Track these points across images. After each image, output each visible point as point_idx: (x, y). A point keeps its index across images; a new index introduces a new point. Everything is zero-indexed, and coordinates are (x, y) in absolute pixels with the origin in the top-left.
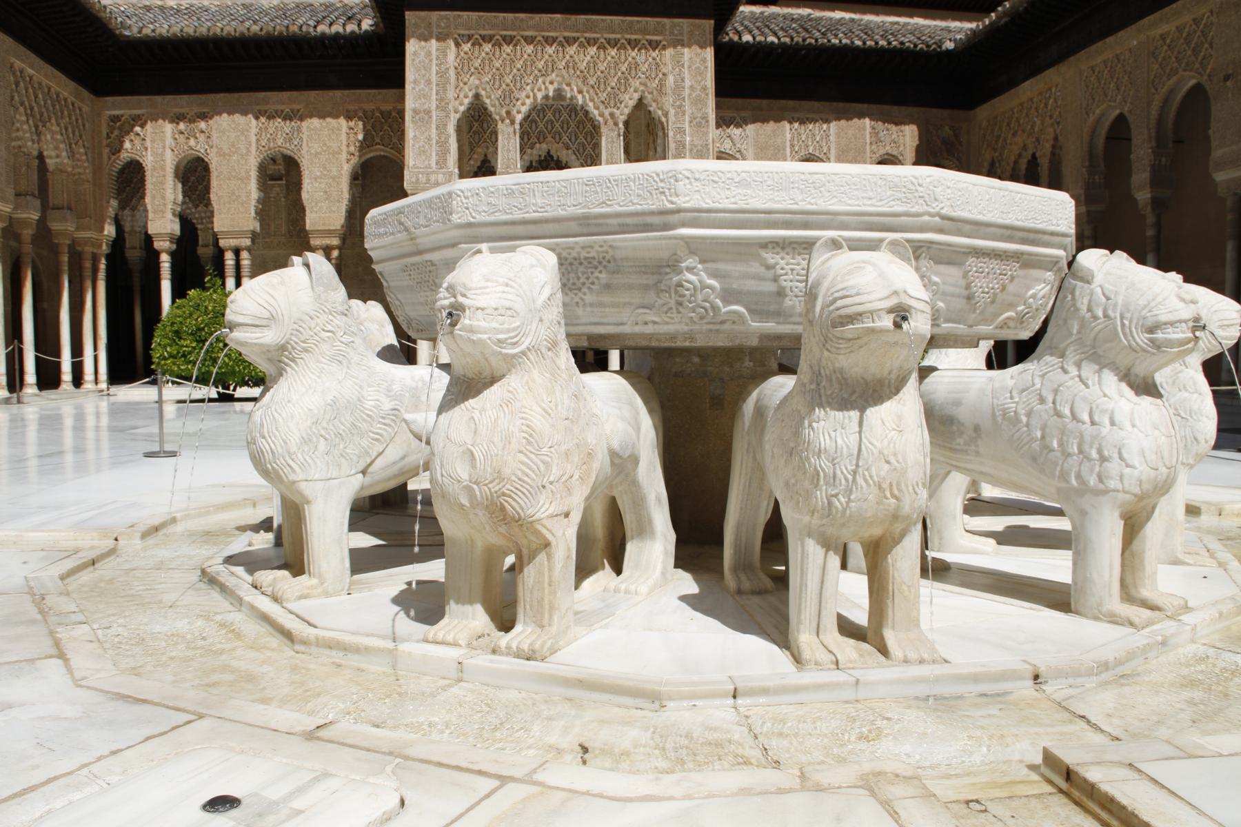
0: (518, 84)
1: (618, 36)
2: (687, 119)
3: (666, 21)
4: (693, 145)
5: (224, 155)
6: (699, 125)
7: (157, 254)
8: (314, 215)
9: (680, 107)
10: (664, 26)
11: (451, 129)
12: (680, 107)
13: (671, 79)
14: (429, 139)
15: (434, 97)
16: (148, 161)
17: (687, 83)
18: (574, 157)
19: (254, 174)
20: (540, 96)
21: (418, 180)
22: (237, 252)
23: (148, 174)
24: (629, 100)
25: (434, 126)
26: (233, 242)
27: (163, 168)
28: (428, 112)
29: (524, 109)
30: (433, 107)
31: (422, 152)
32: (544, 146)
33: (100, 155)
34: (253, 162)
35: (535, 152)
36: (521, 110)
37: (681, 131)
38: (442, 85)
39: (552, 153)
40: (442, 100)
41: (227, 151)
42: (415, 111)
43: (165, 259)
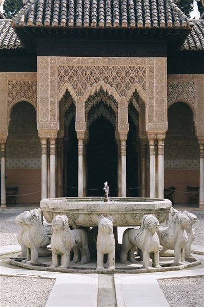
0: (84, 86)
3: (147, 59)
4: (157, 111)
6: (160, 103)
10: (145, 61)
11: (56, 105)
12: (152, 95)
13: (148, 84)
14: (47, 109)
15: (49, 92)
17: (155, 85)
18: (113, 103)
20: (93, 91)
24: (130, 93)
25: (49, 104)
28: (47, 98)
29: (87, 97)
30: (49, 96)
32: (99, 98)
37: (152, 105)
39: (103, 100)
40: (52, 94)
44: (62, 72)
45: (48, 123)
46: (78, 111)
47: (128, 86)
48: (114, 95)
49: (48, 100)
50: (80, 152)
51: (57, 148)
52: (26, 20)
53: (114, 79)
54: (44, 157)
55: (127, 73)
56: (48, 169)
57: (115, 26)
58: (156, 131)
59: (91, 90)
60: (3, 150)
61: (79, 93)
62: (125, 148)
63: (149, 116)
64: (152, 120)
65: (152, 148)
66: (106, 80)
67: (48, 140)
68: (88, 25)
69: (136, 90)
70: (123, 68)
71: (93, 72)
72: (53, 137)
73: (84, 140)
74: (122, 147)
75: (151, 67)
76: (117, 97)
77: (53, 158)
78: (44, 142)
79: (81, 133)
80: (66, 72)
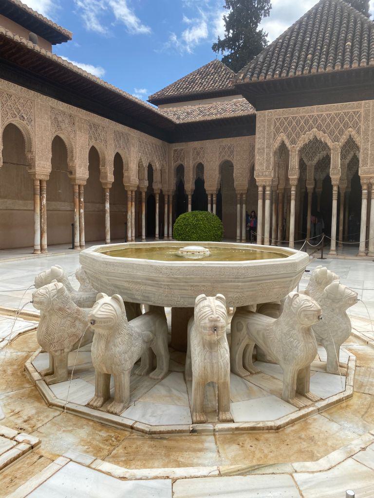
1: (341, 111)
2: (370, 144)
5: (208, 162)
7: (187, 196)
8: (237, 183)
9: (367, 138)
11: (271, 155)
14: (263, 159)
16: (185, 164)
19: (217, 169)
21: (259, 174)
22: (212, 195)
23: (185, 169)
24: (343, 139)
26: (210, 192)
27: (190, 167)
28: (263, 149)
31: (261, 164)
32: (325, 152)
33: (171, 163)
34: (218, 163)
35: (321, 155)
36: (300, 144)
37: (366, 149)
38: (269, 139)
41: (209, 160)
42: (259, 149)
43: (190, 197)
44: (278, 124)
45: (265, 175)
46: (291, 159)
47: (341, 132)
48: (327, 142)
49: (264, 151)
50: (293, 197)
51: (271, 194)
52: (244, 78)
53: (328, 126)
54: (260, 202)
55: (342, 119)
56: (265, 211)
57: (327, 70)
58: (368, 175)
59: (305, 138)
60: (244, 199)
61: (293, 142)
62: (336, 192)
63: (363, 160)
64: (365, 164)
65: (365, 192)
66: (319, 128)
67: (264, 188)
68: (300, 73)
69: (350, 136)
70: (337, 115)
71: (306, 122)
72: (268, 184)
73: (297, 186)
74: (334, 192)
75: (368, 110)
76: (330, 143)
77: (268, 202)
78: (260, 189)
79: (293, 179)
80: (282, 123)
